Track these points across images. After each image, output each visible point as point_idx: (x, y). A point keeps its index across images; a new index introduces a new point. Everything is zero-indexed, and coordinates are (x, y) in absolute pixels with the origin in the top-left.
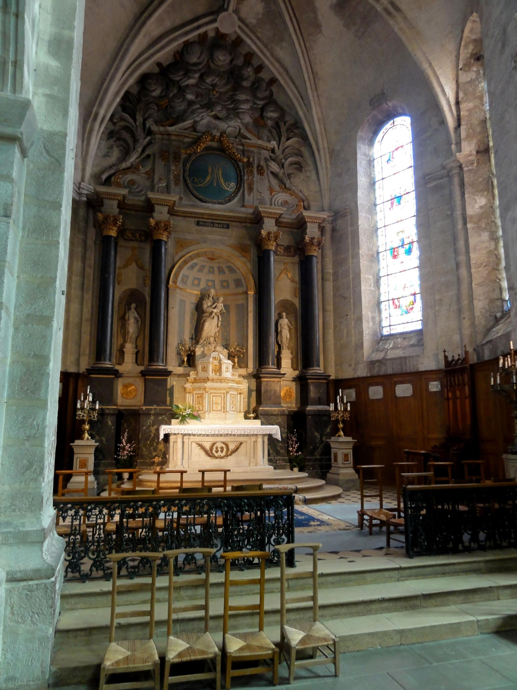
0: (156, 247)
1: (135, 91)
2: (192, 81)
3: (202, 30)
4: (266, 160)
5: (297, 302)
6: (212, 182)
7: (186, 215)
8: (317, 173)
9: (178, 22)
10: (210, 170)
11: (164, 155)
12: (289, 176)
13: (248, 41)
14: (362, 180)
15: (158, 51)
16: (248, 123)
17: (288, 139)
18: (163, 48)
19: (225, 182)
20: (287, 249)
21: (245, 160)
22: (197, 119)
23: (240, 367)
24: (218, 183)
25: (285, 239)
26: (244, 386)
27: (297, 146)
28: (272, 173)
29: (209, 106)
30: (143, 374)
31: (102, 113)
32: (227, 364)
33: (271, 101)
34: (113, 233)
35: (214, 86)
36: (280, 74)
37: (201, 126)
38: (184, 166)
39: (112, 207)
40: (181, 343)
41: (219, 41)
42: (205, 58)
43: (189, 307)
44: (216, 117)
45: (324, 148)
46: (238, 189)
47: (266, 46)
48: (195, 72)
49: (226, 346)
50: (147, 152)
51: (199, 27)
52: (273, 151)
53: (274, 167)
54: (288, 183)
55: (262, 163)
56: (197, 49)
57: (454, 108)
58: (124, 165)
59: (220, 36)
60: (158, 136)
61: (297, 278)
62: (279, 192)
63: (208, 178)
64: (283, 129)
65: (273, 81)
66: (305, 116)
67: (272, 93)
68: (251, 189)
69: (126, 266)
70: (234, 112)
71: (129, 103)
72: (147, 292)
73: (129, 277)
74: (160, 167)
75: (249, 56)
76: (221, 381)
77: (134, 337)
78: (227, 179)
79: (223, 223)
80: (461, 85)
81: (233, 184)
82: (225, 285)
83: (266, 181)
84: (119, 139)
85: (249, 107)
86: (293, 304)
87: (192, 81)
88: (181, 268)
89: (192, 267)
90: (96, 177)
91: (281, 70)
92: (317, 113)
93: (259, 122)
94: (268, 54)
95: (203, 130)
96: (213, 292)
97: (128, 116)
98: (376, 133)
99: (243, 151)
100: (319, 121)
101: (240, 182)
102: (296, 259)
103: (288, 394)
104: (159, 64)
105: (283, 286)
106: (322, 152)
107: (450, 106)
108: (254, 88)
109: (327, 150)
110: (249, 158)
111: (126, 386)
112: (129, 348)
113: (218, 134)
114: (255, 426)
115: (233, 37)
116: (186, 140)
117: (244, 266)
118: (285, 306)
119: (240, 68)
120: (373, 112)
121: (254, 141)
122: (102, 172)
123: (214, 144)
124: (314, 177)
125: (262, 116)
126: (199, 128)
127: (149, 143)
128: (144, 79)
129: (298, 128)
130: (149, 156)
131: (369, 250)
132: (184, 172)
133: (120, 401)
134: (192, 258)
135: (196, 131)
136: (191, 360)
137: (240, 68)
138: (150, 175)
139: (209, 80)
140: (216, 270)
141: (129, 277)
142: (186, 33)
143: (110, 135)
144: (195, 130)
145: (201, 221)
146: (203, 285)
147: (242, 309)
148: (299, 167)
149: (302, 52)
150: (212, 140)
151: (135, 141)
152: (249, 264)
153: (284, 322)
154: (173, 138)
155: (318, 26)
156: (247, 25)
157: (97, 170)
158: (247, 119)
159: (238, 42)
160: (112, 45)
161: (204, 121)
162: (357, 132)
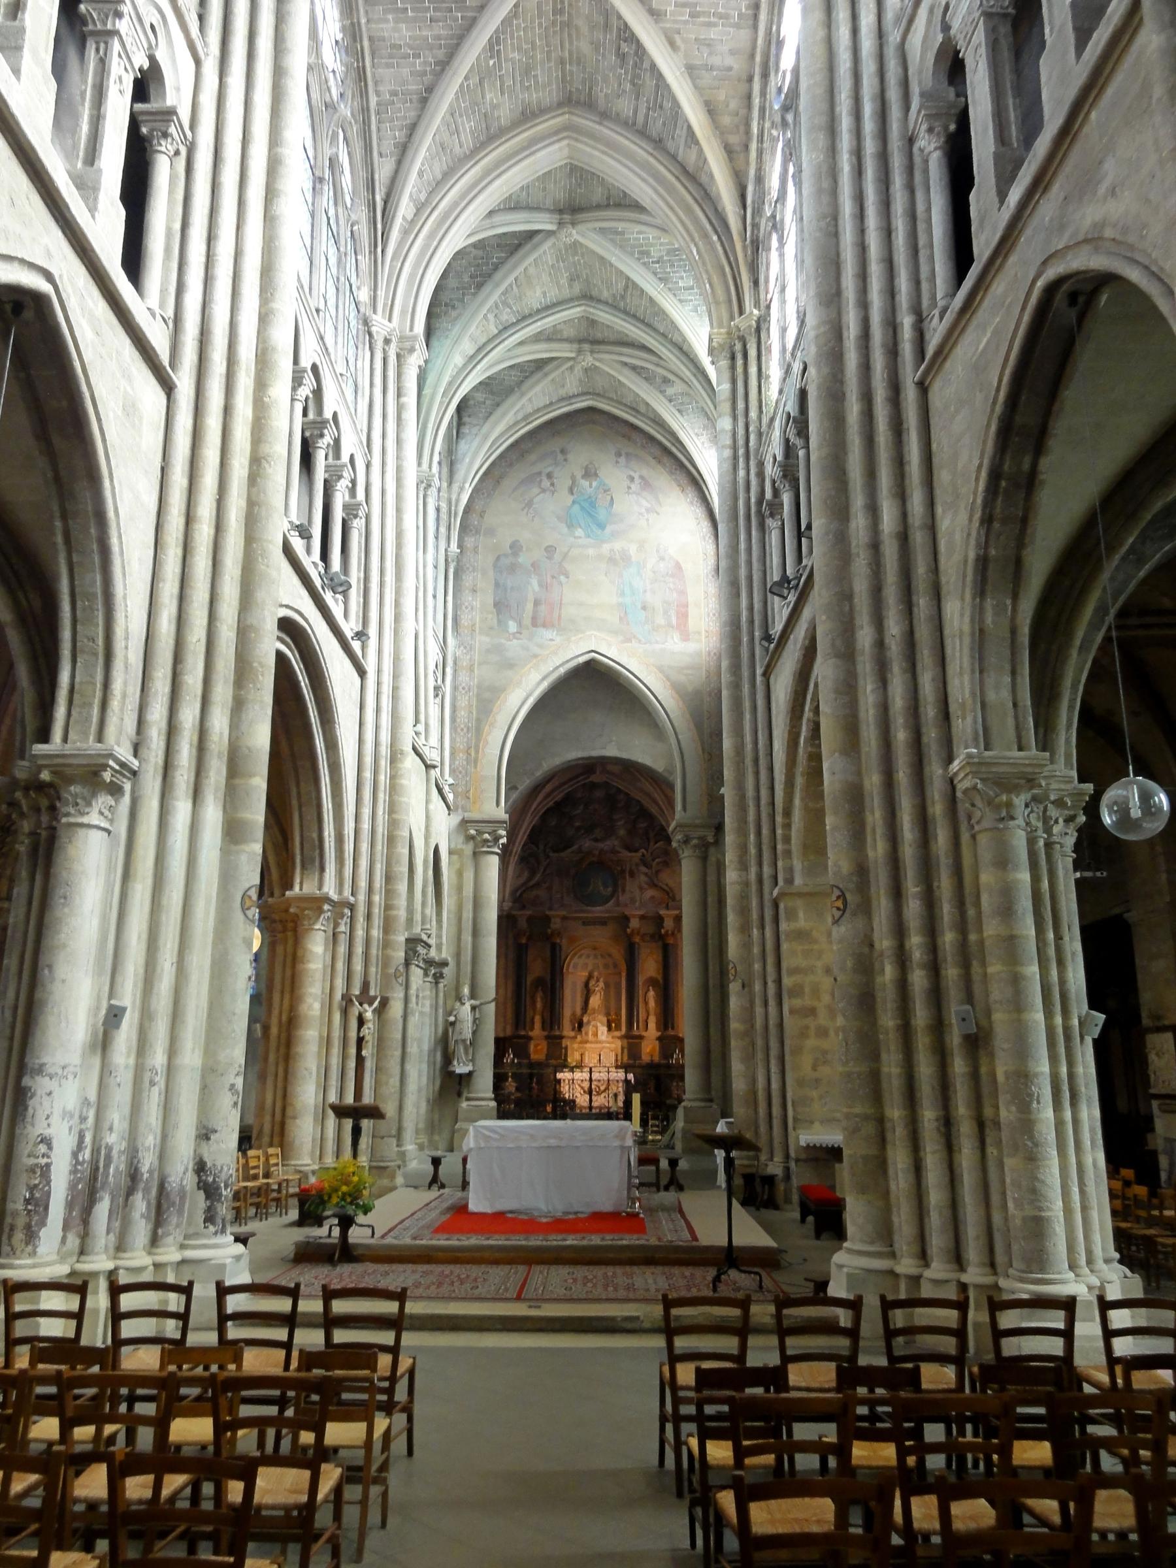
0: (555, 948)
2: (578, 811)
5: (660, 978)
7: (575, 919)
12: (657, 872)
20: (652, 936)
25: (651, 929)
26: (619, 1043)
30: (547, 1038)
32: (603, 1029)
34: (524, 941)
39: (523, 924)
40: (574, 1014)
41: (594, 786)
43: (580, 987)
44: (596, 840)
46: (614, 892)
49: (608, 1014)
53: (643, 869)
61: (660, 958)
64: (652, 835)
68: (624, 891)
72: (548, 978)
73: (536, 969)
76: (597, 1042)
78: (606, 886)
79: (603, 922)
81: (610, 889)
82: (606, 966)
87: (578, 811)
89: (580, 956)
96: (596, 974)
101: (615, 886)
102: (660, 943)
103: (654, 1048)
105: (649, 966)
111: (536, 1046)
112: (538, 1019)
113: (597, 852)
114: (621, 1075)
117: (618, 953)
133: (532, 1056)
136: (580, 1026)
141: (536, 969)
143: (523, 860)
146: (590, 968)
147: (618, 985)
148: (666, 864)
153: (651, 993)
157: (516, 890)
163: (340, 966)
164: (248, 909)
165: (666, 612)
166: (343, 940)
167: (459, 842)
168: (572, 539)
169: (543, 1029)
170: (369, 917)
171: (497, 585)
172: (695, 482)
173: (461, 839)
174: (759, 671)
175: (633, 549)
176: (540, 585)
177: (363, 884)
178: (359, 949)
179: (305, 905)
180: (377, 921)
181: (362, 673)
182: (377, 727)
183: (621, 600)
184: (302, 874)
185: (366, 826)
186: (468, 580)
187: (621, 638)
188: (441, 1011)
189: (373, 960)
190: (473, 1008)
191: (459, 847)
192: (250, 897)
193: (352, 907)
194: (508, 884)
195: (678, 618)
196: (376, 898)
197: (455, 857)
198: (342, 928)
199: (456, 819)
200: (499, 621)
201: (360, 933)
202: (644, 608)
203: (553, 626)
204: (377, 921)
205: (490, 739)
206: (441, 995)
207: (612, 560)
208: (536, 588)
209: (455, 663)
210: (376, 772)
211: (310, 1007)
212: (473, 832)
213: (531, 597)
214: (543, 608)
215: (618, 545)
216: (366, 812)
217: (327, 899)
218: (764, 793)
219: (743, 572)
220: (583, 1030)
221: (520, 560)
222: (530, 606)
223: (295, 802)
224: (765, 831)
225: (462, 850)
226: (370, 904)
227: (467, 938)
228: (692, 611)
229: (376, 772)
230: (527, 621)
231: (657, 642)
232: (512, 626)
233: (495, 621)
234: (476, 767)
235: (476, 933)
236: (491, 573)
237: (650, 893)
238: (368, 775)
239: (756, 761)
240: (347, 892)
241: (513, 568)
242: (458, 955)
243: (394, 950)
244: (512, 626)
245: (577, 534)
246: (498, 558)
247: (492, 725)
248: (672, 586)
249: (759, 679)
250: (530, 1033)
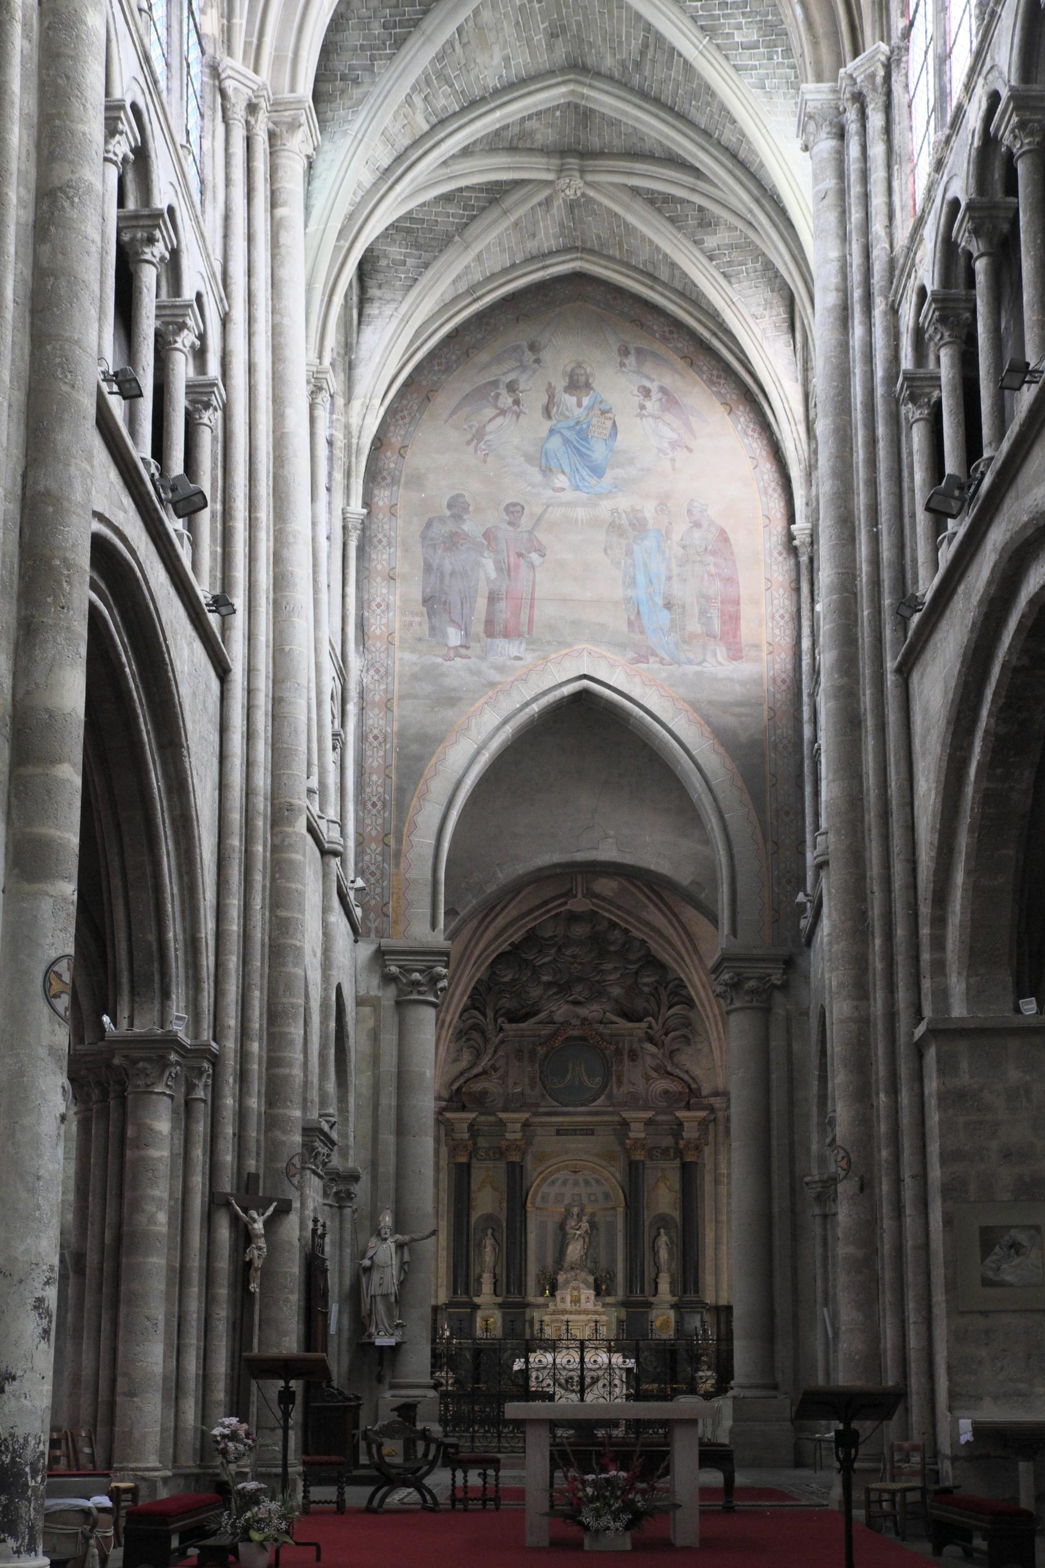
5: (676, 1215)
17: (670, 1008)
21: (613, 1047)
22: (554, 1009)
23: (609, 1294)
32: (587, 1294)
35: (574, 957)
37: (558, 1017)
41: (573, 918)
44: (576, 1003)
45: (715, 1016)
53: (650, 1048)
55: (635, 1046)
61: (677, 1186)
68: (620, 1082)
69: (480, 1189)
72: (503, 1217)
77: (491, 1265)
81: (598, 1079)
86: (673, 1218)
88: (539, 1186)
109: (719, 1018)
117: (613, 1177)
118: (663, 1222)
134: (551, 1174)
140: (582, 1183)
148: (687, 1040)
152: (618, 1175)
163: (198, 1153)
164: (57, 996)
165: (703, 613)
166: (201, 1111)
167: (372, 985)
168: (549, 493)
169: (495, 1293)
170: (243, 1077)
171: (428, 568)
172: (749, 397)
173: (375, 981)
174: (890, 665)
175: (649, 510)
176: (499, 569)
177: (232, 1021)
178: (229, 1130)
179: (135, 1054)
180: (256, 1085)
181: (223, 672)
182: (249, 764)
183: (630, 593)
184: (132, 1002)
185: (234, 927)
186: (380, 559)
187: (631, 654)
188: (348, 1250)
189: (252, 1145)
190: (400, 1246)
191: (372, 993)
192: (59, 976)
193: (216, 1060)
195: (724, 623)
196: (255, 1047)
197: (367, 1010)
198: (200, 1093)
199: (366, 950)
200: (432, 629)
201: (229, 1102)
202: (668, 606)
203: (520, 635)
204: (256, 1085)
205: (420, 819)
206: (348, 1226)
207: (614, 527)
208: (493, 574)
209: (362, 696)
210: (248, 839)
211: (152, 1219)
212: (394, 969)
213: (483, 590)
214: (502, 605)
215: (623, 502)
216: (234, 903)
217: (172, 1042)
218: (898, 868)
219: (861, 500)
220: (558, 1293)
221: (466, 527)
222: (482, 603)
223: (117, 883)
224: (900, 932)
225: (378, 998)
226: (243, 1055)
227: (388, 1139)
228: (747, 611)
229: (248, 839)
230: (478, 628)
231: (690, 662)
232: (454, 637)
233: (426, 627)
234: (397, 865)
235: (401, 1129)
236: (418, 550)
238: (235, 842)
239: (885, 815)
240: (206, 1035)
241: (453, 541)
242: (374, 1164)
243: (284, 1132)
244: (454, 637)
245: (558, 485)
246: (429, 524)
247: (423, 797)
248: (712, 569)
249: (890, 678)
250: (476, 1300)
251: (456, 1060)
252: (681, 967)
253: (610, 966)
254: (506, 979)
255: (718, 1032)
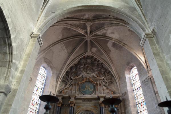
1: (69, 71)
2: (82, 66)
3: (83, 56)
4: (101, 82)
6: (87, 90)
8: (117, 84)
9: (78, 55)
10: (86, 87)
11: (75, 85)
13: (94, 56)
14: (128, 84)
15: (74, 62)
16: (97, 74)
17: (107, 76)
18: (74, 61)
19: (90, 89)
24: (88, 90)
27: (110, 77)
28: (104, 85)
29: (86, 71)
31: (61, 76)
33: (102, 67)
36: (103, 61)
38: (80, 86)
41: (88, 57)
42: (85, 61)
44: (88, 74)
45: (117, 77)
47: (99, 56)
48: (83, 64)
50: (71, 84)
51: (83, 55)
52: (103, 79)
53: (104, 83)
54: (108, 87)
56: (83, 60)
57: (145, 63)
58: (65, 88)
59: (88, 56)
60: (74, 80)
62: (105, 90)
63: (86, 89)
64: (106, 74)
65: (102, 63)
66: (111, 70)
67: (102, 66)
68: (97, 90)
70: (93, 72)
71: (67, 73)
74: (74, 87)
75: (96, 59)
80: (146, 58)
81: (92, 89)
83: (102, 87)
84: (65, 82)
85: (96, 70)
87: (82, 66)
90: (58, 91)
91: (103, 61)
92: (114, 69)
93: (99, 73)
94: (99, 58)
95: (85, 77)
97: (67, 76)
98: (130, 71)
99: (95, 81)
100: (115, 70)
101: (94, 88)
104: (75, 64)
106: (117, 78)
107: (144, 63)
108: (98, 66)
110: (97, 82)
113: (88, 78)
115: (91, 56)
116: (81, 80)
119: (94, 62)
120: (128, 67)
121: (98, 78)
122: (60, 90)
123: (88, 80)
124: (116, 85)
125: (100, 72)
126: (83, 77)
127: (72, 82)
128: (71, 68)
129: (110, 73)
130: (71, 85)
131: (133, 104)
132: (80, 88)
135: (83, 77)
137: (94, 62)
138: (71, 89)
139: (86, 66)
142: (80, 57)
143: (63, 81)
144: (83, 77)
145: (84, 100)
148: (111, 83)
149: (107, 56)
150: (87, 79)
151: (68, 82)
152: (97, 111)
154: (77, 80)
155: (110, 50)
156: (93, 53)
157: (59, 90)
158: (96, 73)
159: (92, 57)
160: (63, 62)
161: (85, 75)
162: (125, 72)
194: (57, 88)
237: (107, 91)
251: (62, 86)
252: (109, 67)
253: (95, 68)
254: (74, 70)
255: (118, 80)
